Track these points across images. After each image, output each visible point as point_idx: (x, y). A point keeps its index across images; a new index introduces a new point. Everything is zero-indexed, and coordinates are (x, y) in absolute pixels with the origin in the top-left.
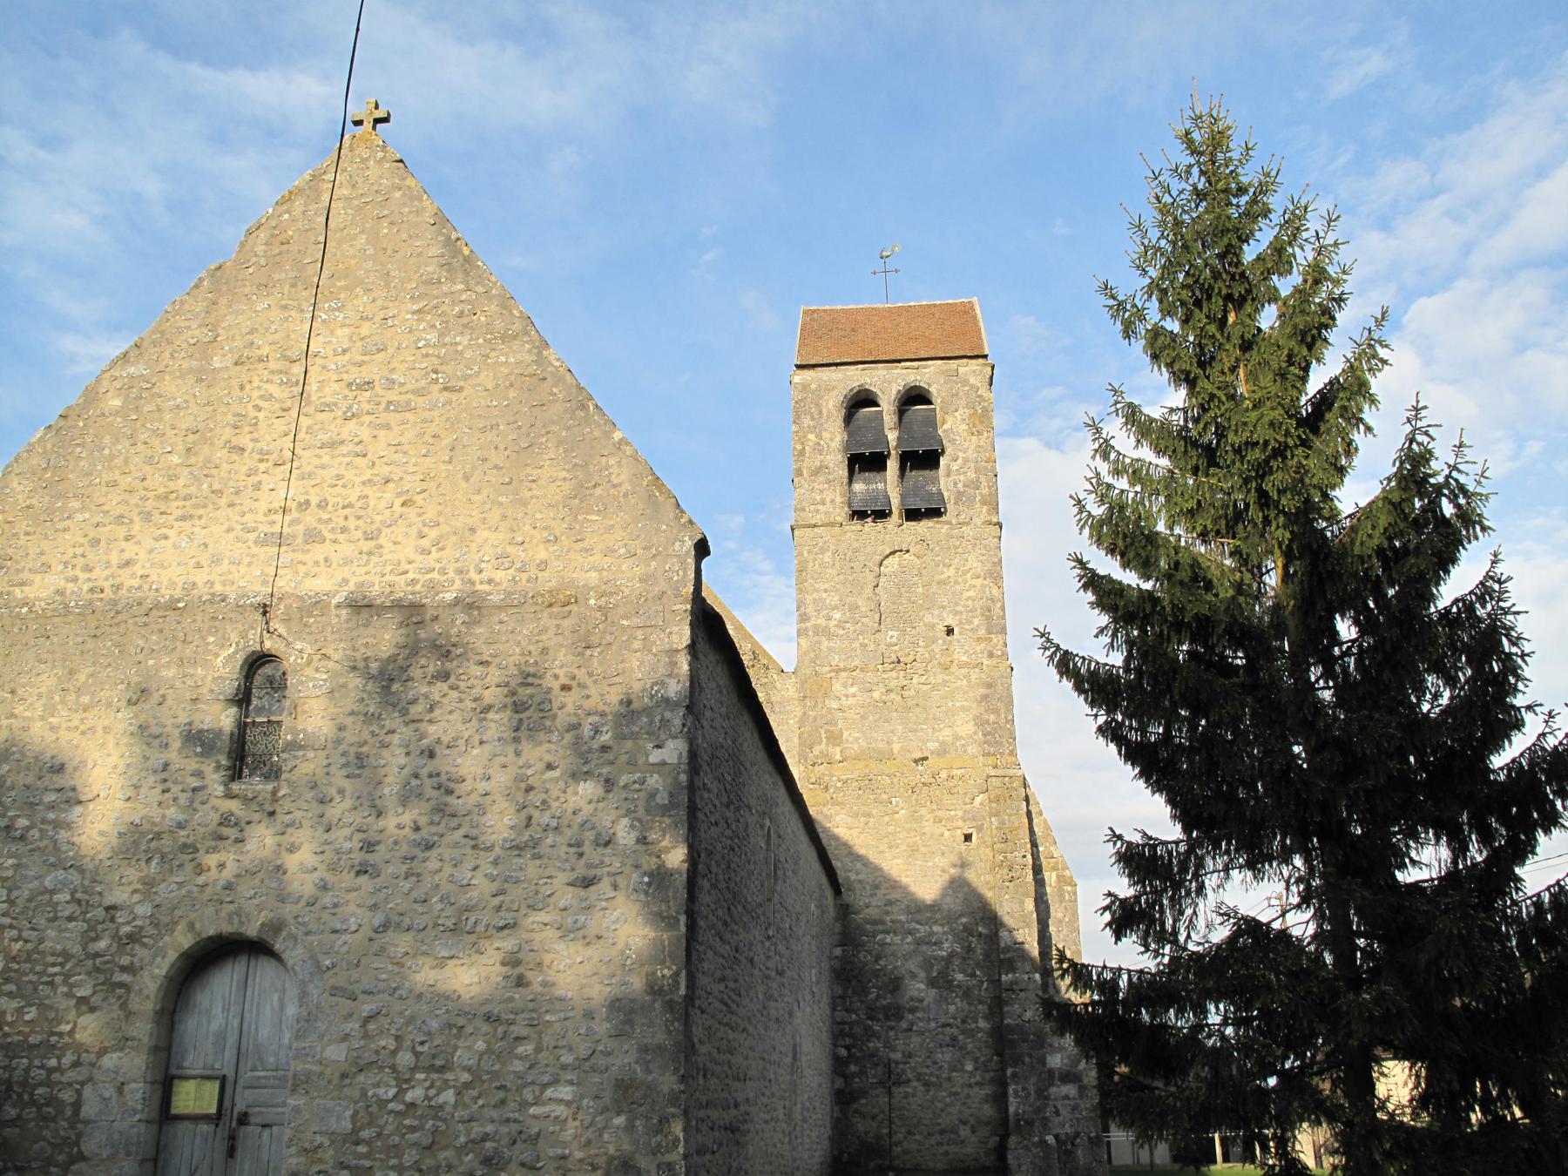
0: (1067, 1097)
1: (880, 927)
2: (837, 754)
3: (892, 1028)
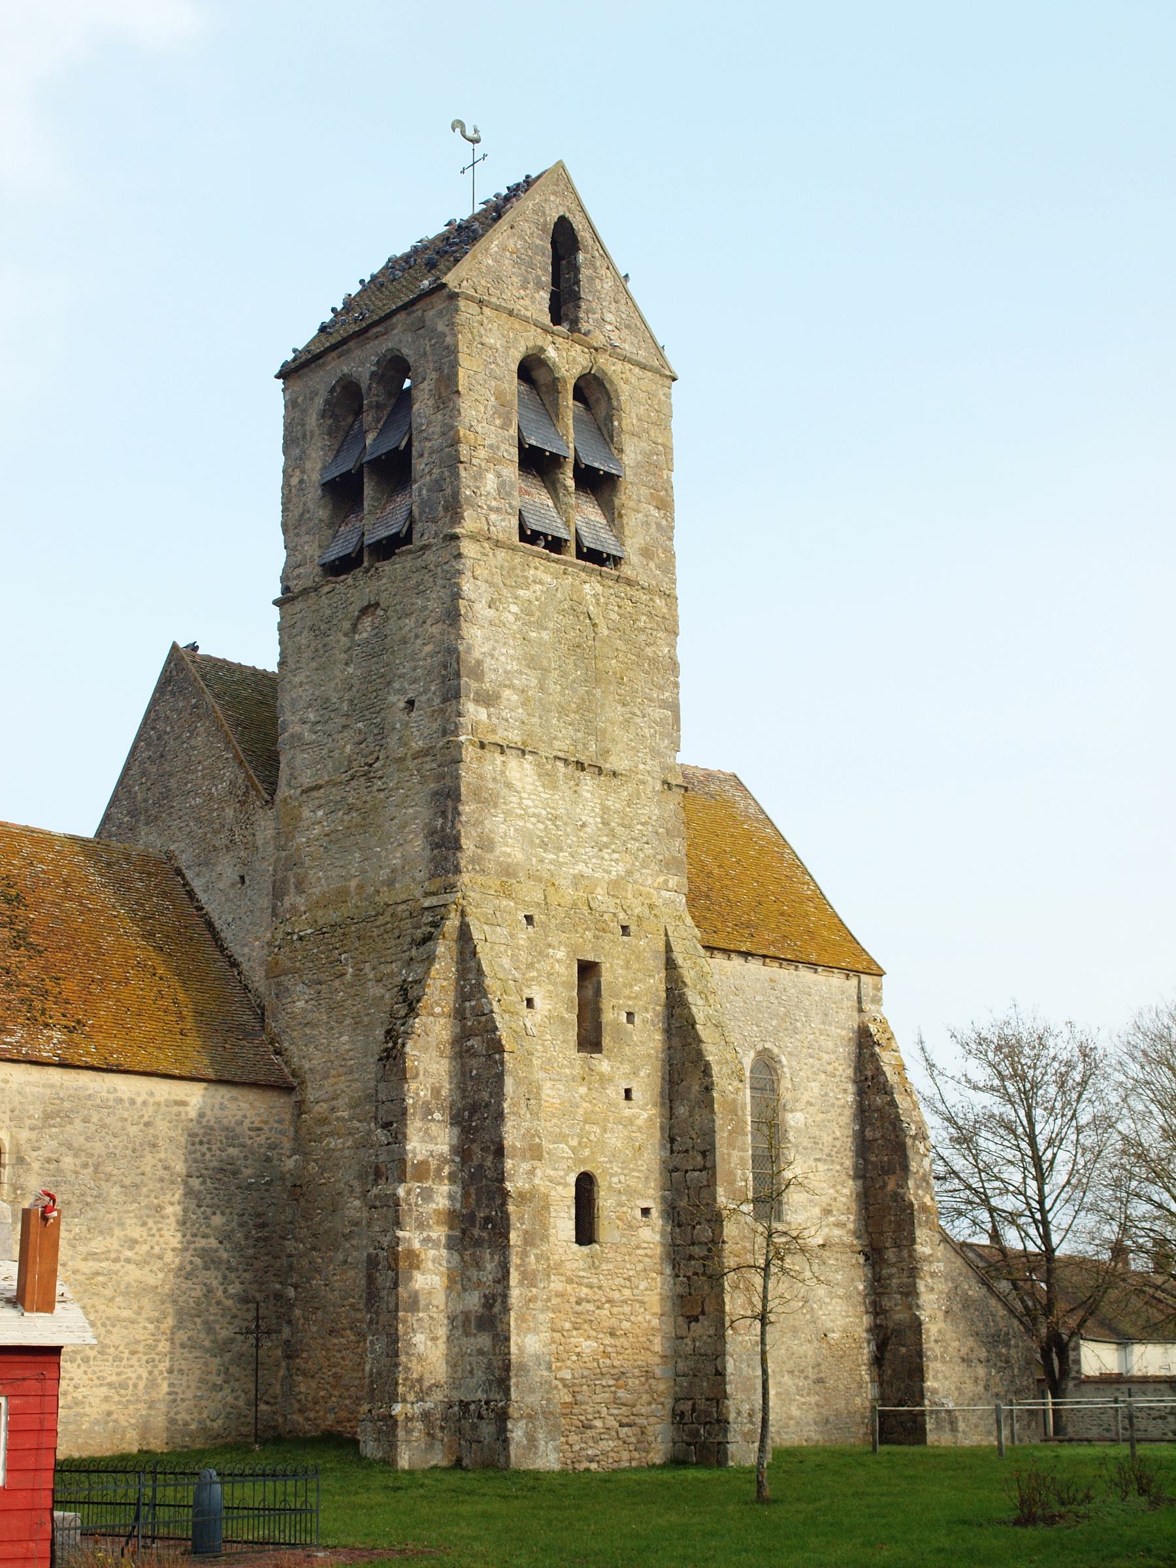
0: (480, 1352)
1: (326, 1129)
2: (301, 902)
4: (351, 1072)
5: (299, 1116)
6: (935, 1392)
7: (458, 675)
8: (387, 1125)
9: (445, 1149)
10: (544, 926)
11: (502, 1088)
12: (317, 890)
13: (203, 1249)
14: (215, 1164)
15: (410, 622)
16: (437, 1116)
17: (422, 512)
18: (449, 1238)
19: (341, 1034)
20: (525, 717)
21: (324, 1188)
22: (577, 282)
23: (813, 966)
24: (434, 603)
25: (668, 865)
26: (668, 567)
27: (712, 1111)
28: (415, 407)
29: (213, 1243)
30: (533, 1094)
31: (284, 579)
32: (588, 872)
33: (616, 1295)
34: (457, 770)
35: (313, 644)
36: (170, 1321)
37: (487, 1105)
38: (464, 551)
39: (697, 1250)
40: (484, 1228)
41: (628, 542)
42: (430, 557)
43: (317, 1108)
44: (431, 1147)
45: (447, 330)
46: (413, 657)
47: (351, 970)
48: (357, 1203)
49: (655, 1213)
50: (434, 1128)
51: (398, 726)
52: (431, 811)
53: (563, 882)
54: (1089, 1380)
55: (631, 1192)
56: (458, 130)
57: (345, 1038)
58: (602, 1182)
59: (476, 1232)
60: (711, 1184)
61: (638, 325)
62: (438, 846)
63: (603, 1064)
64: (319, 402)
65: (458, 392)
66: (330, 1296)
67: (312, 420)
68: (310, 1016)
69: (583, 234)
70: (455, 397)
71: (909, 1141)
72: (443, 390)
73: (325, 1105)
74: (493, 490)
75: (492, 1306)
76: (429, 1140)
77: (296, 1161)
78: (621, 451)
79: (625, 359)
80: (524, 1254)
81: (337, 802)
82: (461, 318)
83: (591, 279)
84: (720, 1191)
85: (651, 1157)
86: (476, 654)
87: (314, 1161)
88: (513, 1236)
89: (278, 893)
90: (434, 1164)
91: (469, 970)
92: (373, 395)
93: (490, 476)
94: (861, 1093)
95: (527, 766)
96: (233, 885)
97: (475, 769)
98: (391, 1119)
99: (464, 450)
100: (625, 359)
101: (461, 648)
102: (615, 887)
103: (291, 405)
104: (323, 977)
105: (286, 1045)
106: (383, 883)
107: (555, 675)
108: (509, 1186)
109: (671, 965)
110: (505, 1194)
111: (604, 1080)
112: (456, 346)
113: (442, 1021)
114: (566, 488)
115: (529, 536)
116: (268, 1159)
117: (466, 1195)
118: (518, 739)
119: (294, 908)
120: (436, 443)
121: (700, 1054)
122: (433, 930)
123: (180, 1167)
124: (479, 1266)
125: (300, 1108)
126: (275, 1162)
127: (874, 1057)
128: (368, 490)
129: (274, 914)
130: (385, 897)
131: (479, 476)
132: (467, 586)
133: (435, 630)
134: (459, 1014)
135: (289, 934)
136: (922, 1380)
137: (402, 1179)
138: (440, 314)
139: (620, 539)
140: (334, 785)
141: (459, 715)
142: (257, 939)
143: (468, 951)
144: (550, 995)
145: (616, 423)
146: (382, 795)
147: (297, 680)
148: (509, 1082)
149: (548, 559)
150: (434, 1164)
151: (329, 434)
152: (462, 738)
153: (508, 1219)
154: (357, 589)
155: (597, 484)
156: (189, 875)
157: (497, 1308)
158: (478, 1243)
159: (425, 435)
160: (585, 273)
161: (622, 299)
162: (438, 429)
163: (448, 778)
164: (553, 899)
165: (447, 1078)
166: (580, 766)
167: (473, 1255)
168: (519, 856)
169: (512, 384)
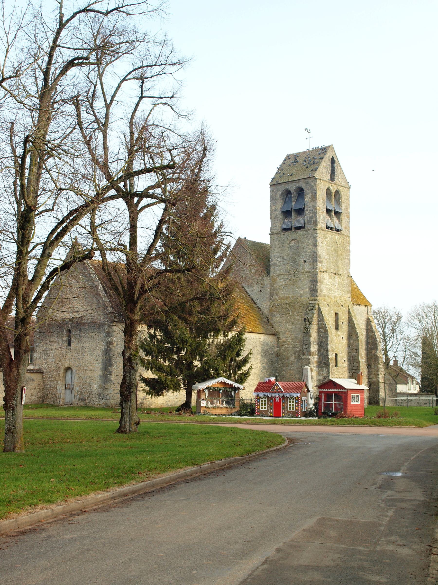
6: (381, 395)
7: (317, 257)
9: (316, 349)
15: (305, 245)
22: (334, 170)
23: (359, 305)
24: (311, 241)
25: (348, 292)
26: (349, 231)
28: (306, 200)
29: (265, 365)
31: (271, 229)
32: (336, 295)
40: (324, 364)
42: (310, 232)
43: (283, 339)
49: (346, 361)
50: (315, 346)
53: (332, 297)
55: (343, 357)
58: (338, 355)
59: (322, 365)
61: (344, 178)
63: (339, 332)
64: (280, 192)
67: (278, 196)
69: (336, 160)
74: (323, 218)
76: (314, 348)
78: (342, 207)
79: (343, 186)
80: (332, 369)
82: (317, 183)
84: (359, 357)
85: (346, 350)
86: (320, 253)
89: (271, 295)
92: (294, 194)
94: (367, 332)
96: (258, 292)
97: (320, 276)
99: (318, 211)
100: (343, 186)
102: (340, 297)
103: (272, 191)
104: (284, 314)
108: (329, 357)
109: (349, 313)
110: (329, 358)
111: (339, 336)
115: (327, 228)
116: (273, 349)
117: (319, 358)
119: (276, 299)
120: (312, 208)
121: (356, 331)
123: (260, 350)
124: (322, 371)
125: (278, 339)
127: (370, 325)
129: (270, 299)
130: (299, 299)
131: (320, 217)
132: (319, 240)
134: (318, 324)
136: (379, 393)
137: (310, 355)
138: (312, 181)
139: (341, 225)
144: (331, 320)
149: (330, 232)
154: (290, 235)
155: (337, 214)
156: (246, 288)
158: (323, 367)
160: (336, 168)
166: (335, 274)
168: (326, 293)
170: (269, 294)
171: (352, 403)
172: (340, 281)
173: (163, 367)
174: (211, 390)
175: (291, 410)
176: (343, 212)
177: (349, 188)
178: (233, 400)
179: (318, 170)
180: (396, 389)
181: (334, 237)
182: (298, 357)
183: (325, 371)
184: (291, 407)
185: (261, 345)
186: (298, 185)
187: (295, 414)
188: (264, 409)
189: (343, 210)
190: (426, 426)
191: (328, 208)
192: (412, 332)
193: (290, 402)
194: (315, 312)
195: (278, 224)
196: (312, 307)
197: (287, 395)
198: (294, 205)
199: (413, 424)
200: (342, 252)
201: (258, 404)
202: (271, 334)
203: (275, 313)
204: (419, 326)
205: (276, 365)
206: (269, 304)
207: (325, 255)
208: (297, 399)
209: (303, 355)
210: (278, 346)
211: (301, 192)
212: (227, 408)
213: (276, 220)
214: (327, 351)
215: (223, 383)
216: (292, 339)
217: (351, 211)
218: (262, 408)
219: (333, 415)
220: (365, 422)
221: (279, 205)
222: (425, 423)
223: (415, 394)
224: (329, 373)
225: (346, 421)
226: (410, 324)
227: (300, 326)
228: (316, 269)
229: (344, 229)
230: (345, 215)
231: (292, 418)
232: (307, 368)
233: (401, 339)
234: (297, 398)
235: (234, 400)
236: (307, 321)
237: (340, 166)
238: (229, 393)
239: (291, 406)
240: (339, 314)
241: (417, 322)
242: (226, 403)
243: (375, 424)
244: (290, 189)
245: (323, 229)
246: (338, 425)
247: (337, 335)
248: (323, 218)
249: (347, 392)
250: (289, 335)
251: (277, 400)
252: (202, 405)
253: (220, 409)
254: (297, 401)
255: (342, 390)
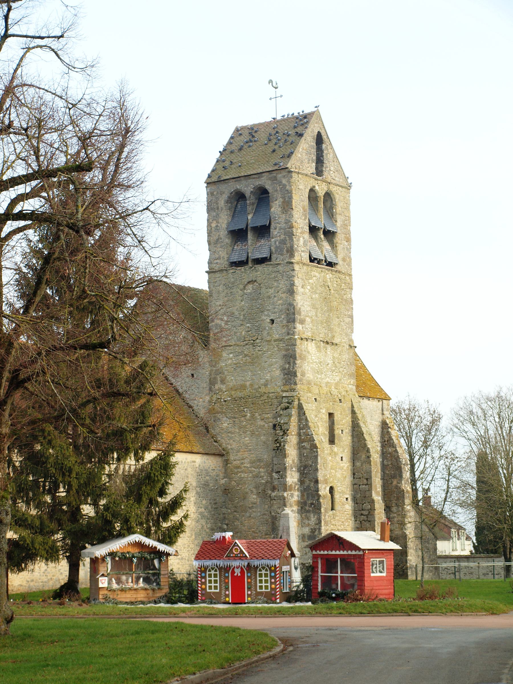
1: (239, 470)
2: (223, 387)
3: (243, 516)
4: (250, 451)
5: (227, 465)
6: (411, 561)
7: (294, 314)
8: (278, 472)
9: (296, 480)
10: (320, 402)
11: (317, 460)
12: (231, 384)
13: (201, 512)
14: (203, 482)
15: (271, 291)
16: (294, 469)
17: (276, 251)
18: (298, 510)
19: (245, 437)
20: (312, 327)
21: (240, 491)
23: (368, 398)
24: (283, 284)
25: (350, 376)
26: (349, 265)
27: (371, 465)
28: (272, 210)
29: (203, 509)
30: (325, 463)
31: (210, 263)
33: (340, 528)
34: (295, 348)
35: (226, 291)
36: (193, 537)
37: (311, 466)
38: (295, 268)
39: (365, 513)
40: (310, 506)
41: (339, 256)
42: (280, 268)
43: (235, 462)
44: (293, 480)
45: (287, 184)
46: (273, 304)
47: (249, 415)
48: (255, 496)
49: (349, 499)
50: (293, 473)
51: (267, 328)
52: (283, 361)
53: (323, 385)
54: (440, 557)
55: (343, 493)
56: (271, 84)
57: (247, 439)
59: (307, 508)
60: (370, 490)
61: (340, 170)
62: (286, 374)
63: (335, 449)
64: (225, 196)
65: (292, 209)
66: (243, 528)
67: (222, 203)
68: (230, 430)
69: (324, 137)
70: (291, 210)
71: (402, 466)
72: (285, 206)
73: (238, 462)
74: (303, 244)
75: (314, 532)
76: (292, 478)
77: (226, 481)
78: (336, 221)
79: (338, 185)
80: (325, 516)
81: (239, 353)
82: (292, 180)
83: (327, 154)
84: (373, 492)
85: (348, 480)
86: (299, 306)
87: (234, 481)
88: (322, 510)
89: (212, 382)
90: (293, 485)
91: (302, 419)
92: (251, 200)
93: (301, 239)
94: (383, 446)
95: (313, 345)
97: (301, 347)
98: (279, 470)
99: (294, 230)
100: (338, 185)
101: (295, 304)
102: (337, 384)
103: (210, 194)
104: (237, 416)
105: (219, 439)
106: (262, 385)
107: (319, 310)
108: (320, 493)
109: (353, 412)
110: (319, 496)
111: (336, 454)
112: (291, 191)
113: (294, 437)
114: (321, 238)
116: (217, 480)
117: (302, 496)
118: (310, 335)
119: (220, 390)
120: (283, 225)
121: (365, 445)
122: (289, 405)
124: (308, 519)
125: (227, 462)
126: (219, 481)
128: (250, 235)
129: (210, 390)
130: (263, 390)
131: (298, 240)
132: (298, 282)
133: (284, 296)
134: (299, 435)
135: (219, 399)
136: (407, 556)
137: (285, 490)
138: (284, 176)
139: (336, 255)
140: (238, 346)
141: (295, 328)
142: (201, 398)
143: (302, 413)
145: (334, 210)
146: (260, 353)
147: (218, 303)
148: (319, 458)
149: (317, 267)
150: (293, 485)
151: (229, 210)
152: (296, 337)
153: (320, 504)
154: (245, 274)
155: (329, 234)
157: (316, 533)
158: (308, 511)
159: (277, 221)
160: (325, 152)
161: (335, 160)
162: (283, 221)
163: (290, 351)
164: (321, 392)
165: (296, 456)
166: (327, 343)
167: (306, 516)
168: (311, 377)
169: (306, 202)
170: (208, 380)
171: (372, 575)
172: (336, 355)
173: (26, 519)
174: (117, 559)
175: (264, 590)
176: (339, 231)
177: (349, 187)
178: (157, 575)
179: (294, 155)
180: (436, 549)
181: (325, 277)
182: (263, 494)
183: (313, 519)
184: (264, 584)
185: (195, 474)
186: (258, 182)
187: (270, 598)
188: (213, 590)
189: (338, 227)
190: (504, 612)
191: (313, 224)
192: (460, 446)
193: (261, 575)
194: (293, 413)
195: (223, 254)
196: (288, 403)
197: (256, 563)
198: (251, 218)
199: (482, 608)
200: (339, 303)
201: (203, 580)
202: (214, 454)
203: (219, 416)
204: (472, 433)
205: (224, 510)
206: (208, 398)
207: (309, 309)
208: (273, 570)
209: (273, 491)
210: (227, 474)
211: (263, 195)
212: (146, 589)
213: (219, 245)
214: (317, 482)
215: (139, 545)
216: (252, 462)
217: (354, 229)
218: (210, 587)
219: (340, 597)
220: (398, 608)
221: (224, 220)
222: (501, 606)
223: (467, 558)
224: (320, 522)
225: (364, 607)
226: (455, 430)
227: (266, 437)
228: (294, 334)
229: (341, 262)
230: (343, 236)
231: (266, 605)
232: (288, 514)
233: (441, 457)
234: (273, 568)
235: (158, 574)
236: (279, 429)
237: (332, 148)
238: (149, 563)
239: (264, 583)
240: (335, 414)
241: (468, 427)
242: (144, 580)
243: (416, 611)
244: (243, 191)
245: (305, 261)
246: (350, 614)
247: (332, 454)
248: (305, 242)
249: (364, 555)
250: (246, 455)
251: (238, 572)
252: (101, 585)
253: (133, 592)
254: (273, 574)
255: (354, 553)
